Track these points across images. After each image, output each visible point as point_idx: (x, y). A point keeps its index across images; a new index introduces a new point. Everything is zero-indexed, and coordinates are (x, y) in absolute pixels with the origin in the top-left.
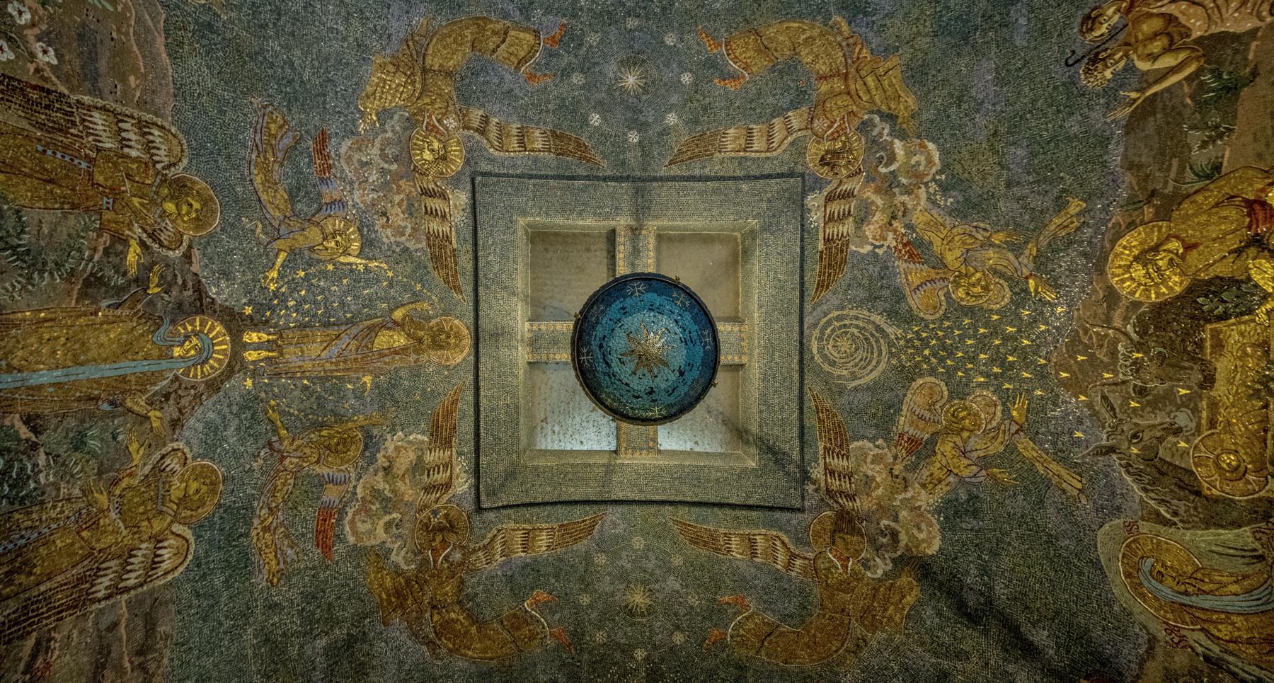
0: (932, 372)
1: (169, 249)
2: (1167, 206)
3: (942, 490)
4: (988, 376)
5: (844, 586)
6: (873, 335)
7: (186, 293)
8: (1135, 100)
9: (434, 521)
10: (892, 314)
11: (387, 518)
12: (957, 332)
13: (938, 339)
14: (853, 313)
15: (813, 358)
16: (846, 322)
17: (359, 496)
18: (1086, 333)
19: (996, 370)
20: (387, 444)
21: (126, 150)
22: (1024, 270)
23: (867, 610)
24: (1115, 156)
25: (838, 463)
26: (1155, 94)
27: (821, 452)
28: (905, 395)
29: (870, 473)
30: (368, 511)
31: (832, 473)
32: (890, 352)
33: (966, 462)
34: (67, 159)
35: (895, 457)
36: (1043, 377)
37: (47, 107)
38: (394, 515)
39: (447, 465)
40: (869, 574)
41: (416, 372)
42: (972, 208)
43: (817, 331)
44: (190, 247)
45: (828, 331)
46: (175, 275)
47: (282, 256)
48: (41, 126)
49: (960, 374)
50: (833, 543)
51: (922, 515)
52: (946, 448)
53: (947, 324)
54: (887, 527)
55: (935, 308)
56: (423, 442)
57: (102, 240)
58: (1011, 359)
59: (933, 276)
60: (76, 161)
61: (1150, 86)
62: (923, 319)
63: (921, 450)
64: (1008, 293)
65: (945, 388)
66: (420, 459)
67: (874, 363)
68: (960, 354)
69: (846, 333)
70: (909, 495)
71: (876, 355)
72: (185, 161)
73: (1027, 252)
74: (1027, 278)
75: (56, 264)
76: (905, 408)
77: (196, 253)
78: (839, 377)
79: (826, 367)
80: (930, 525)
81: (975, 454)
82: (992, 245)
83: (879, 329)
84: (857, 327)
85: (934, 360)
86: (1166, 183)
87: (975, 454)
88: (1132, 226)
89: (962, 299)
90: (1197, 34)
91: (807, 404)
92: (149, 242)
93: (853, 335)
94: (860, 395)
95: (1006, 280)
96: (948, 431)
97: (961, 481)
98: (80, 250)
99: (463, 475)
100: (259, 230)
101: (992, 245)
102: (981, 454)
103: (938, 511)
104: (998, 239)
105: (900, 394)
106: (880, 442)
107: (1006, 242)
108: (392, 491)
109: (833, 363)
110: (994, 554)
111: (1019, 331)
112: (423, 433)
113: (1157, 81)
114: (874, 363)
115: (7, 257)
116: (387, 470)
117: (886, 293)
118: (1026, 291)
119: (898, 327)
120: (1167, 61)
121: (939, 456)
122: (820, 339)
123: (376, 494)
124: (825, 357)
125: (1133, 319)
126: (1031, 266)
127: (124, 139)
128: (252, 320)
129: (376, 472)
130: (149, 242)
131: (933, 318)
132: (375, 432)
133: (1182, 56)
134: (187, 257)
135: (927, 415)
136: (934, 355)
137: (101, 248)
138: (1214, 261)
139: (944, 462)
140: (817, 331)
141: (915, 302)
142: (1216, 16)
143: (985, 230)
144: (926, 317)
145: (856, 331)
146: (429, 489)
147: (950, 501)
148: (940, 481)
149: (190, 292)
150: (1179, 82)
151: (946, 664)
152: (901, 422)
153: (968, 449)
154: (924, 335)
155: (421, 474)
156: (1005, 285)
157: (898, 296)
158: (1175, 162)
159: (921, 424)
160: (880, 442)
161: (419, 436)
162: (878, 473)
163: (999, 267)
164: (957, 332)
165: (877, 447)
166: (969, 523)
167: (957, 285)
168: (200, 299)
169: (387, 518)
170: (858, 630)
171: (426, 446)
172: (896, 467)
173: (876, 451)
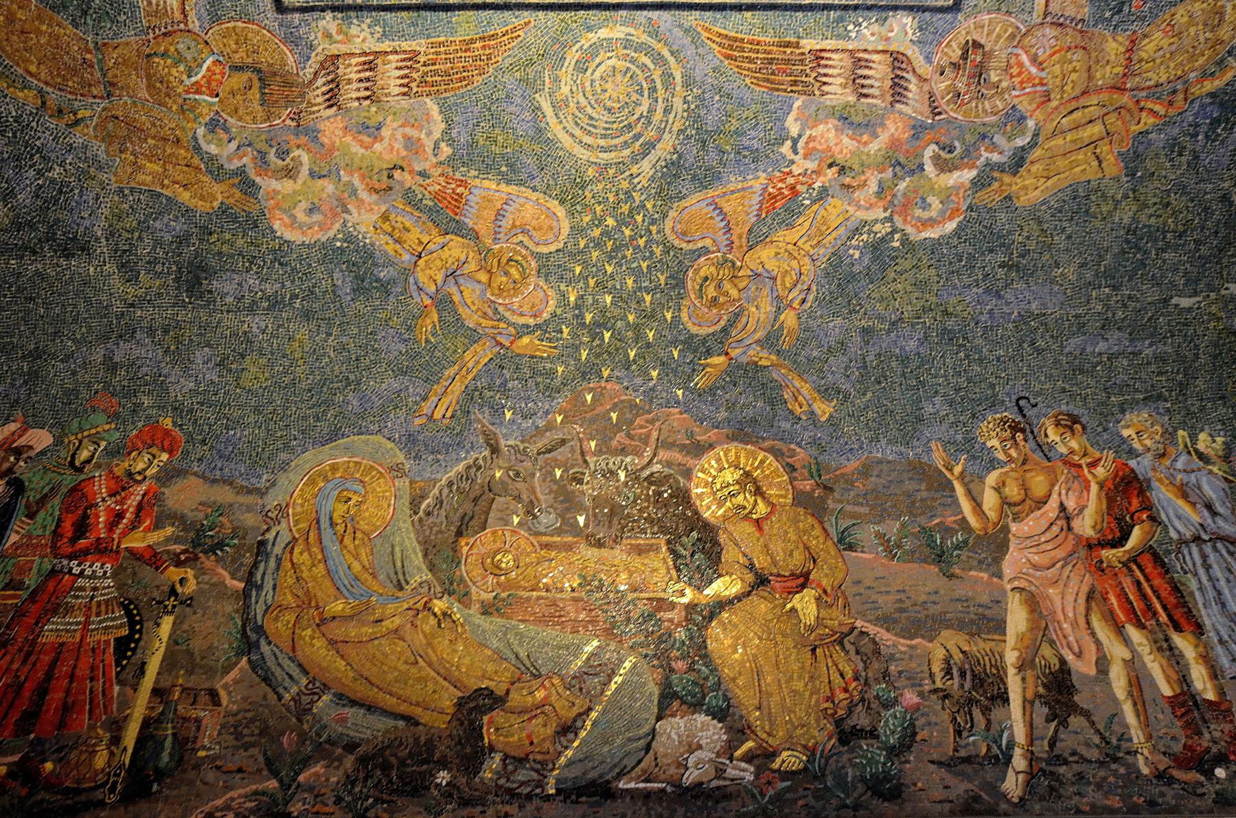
0: (577, 231)
2: (812, 504)
3: (384, 243)
4: (577, 306)
5: (160, 89)
6: (637, 137)
8: (951, 470)
10: (673, 170)
12: (644, 265)
13: (632, 238)
14: (678, 104)
15: (590, 29)
16: (661, 93)
18: (647, 421)
19: (588, 318)
22: (738, 351)
23: (134, 129)
24: (885, 451)
25: (390, 76)
26: (953, 490)
27: (406, 45)
28: (534, 189)
29: (386, 132)
31: (370, 66)
32: (607, 166)
33: (440, 278)
35: (423, 174)
36: (584, 375)
40: (201, 131)
42: (841, 282)
43: (644, 38)
45: (647, 61)
49: (578, 270)
50: (237, 68)
51: (335, 215)
52: (456, 249)
53: (658, 251)
54: (298, 162)
55: (684, 234)
58: (607, 335)
59: (736, 231)
61: (965, 485)
62: (665, 216)
63: (446, 215)
64: (704, 331)
65: (553, 248)
67: (587, 139)
68: (609, 269)
69: (640, 92)
70: (364, 195)
71: (602, 142)
73: (764, 354)
74: (727, 354)
76: (512, 189)
78: (557, 80)
79: (572, 56)
80: (323, 227)
81: (453, 289)
82: (779, 311)
83: (650, 146)
84: (651, 111)
85: (597, 232)
86: (840, 501)
87: (453, 289)
88: (790, 469)
89: (697, 271)
90: (1014, 527)
91: (497, 16)
93: (637, 104)
94: (527, 115)
95: (724, 330)
96: (485, 254)
97: (406, 273)
101: (779, 311)
102: (457, 298)
103: (349, 238)
104: (789, 319)
105: (536, 182)
106: (446, 150)
107: (781, 327)
109: (581, 67)
110: (307, 315)
111: (648, 345)
113: (969, 492)
114: (587, 139)
117: (712, 158)
118: (709, 353)
119: (652, 179)
120: (990, 501)
121: (440, 240)
122: (627, 43)
124: (594, 50)
125: (667, 471)
126: (744, 359)
131: (668, 231)
133: (992, 515)
135: (506, 223)
136: (606, 233)
138: (740, 543)
139: (431, 246)
140: (644, 38)
141: (695, 203)
142: (1028, 543)
143: (804, 301)
144: (668, 224)
145: (644, 108)
147: (371, 256)
148: (397, 241)
150: (961, 512)
151: (103, 248)
152: (486, 183)
153: (461, 281)
154: (639, 218)
156: (718, 327)
157: (706, 178)
158: (864, 510)
159: (490, 214)
160: (446, 150)
162: (388, 147)
163: (744, 320)
164: (644, 265)
165: (436, 146)
166: (343, 282)
167: (720, 265)
170: (91, 110)
172: (407, 176)
173: (429, 144)
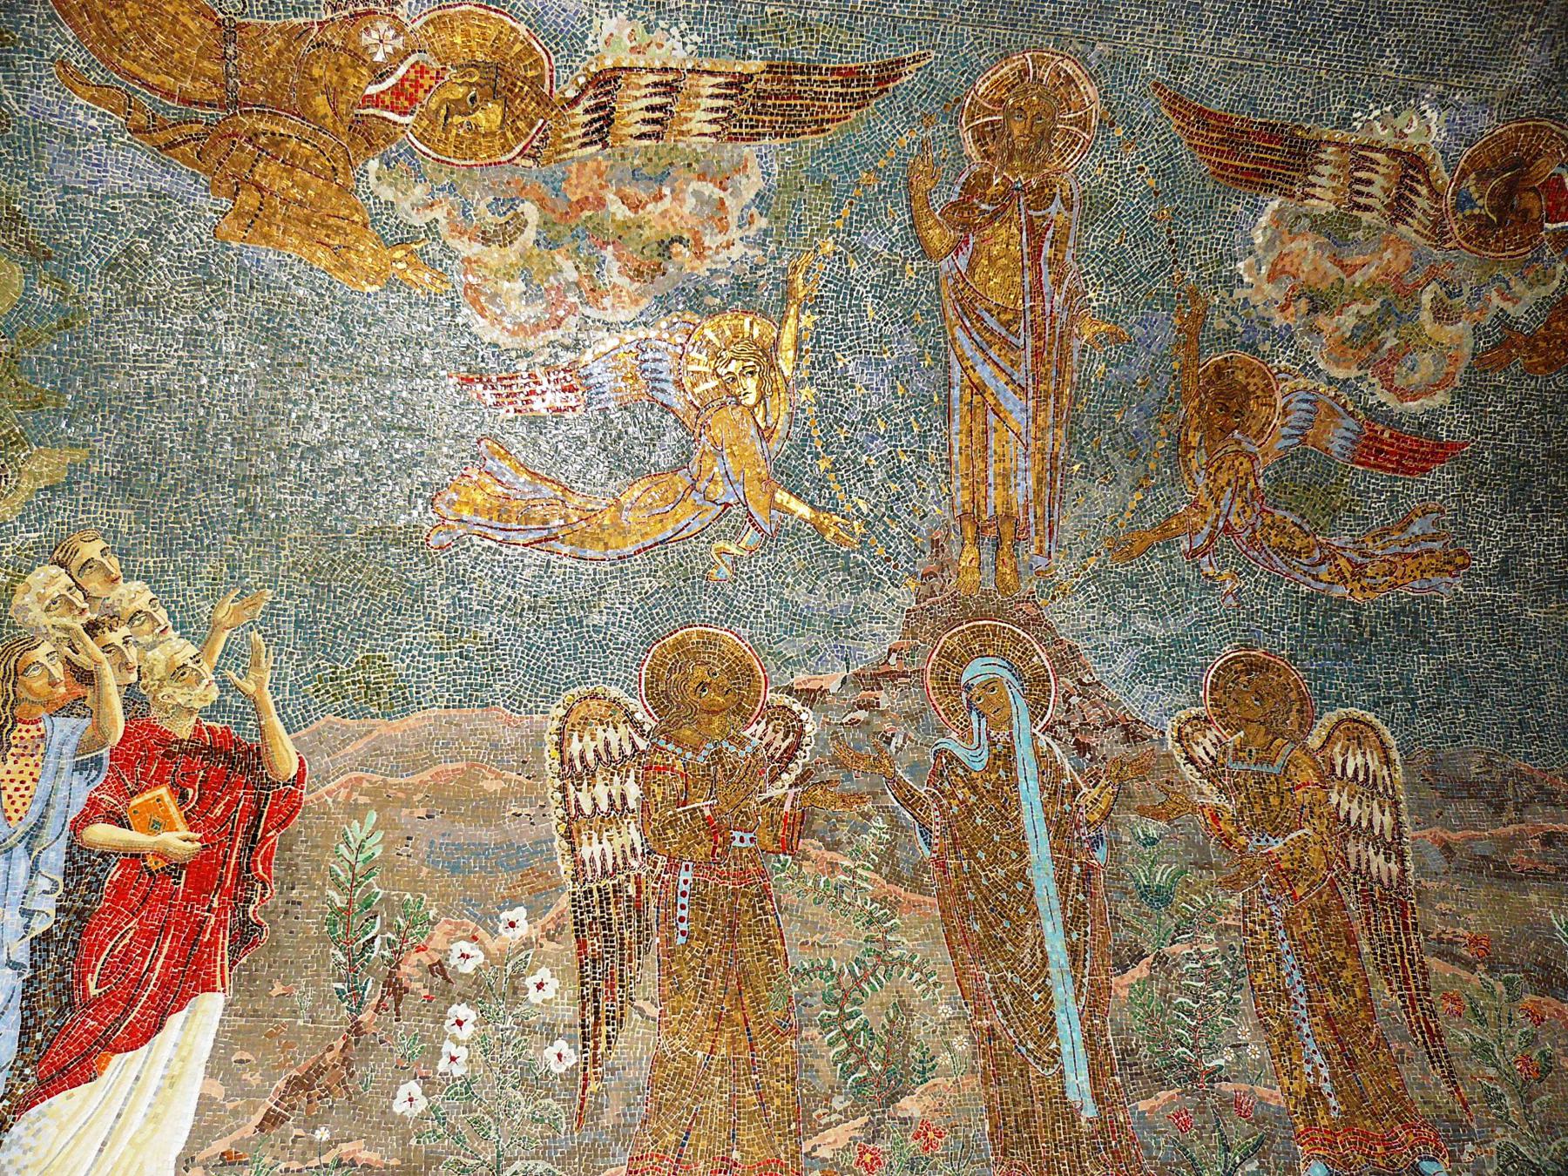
1: (801, 734)
7: (884, 706)
9: (1482, 206)
11: (1426, 316)
17: (1354, 372)
20: (1257, 299)
21: (632, 804)
30: (1395, 357)
34: (685, 901)
37: (607, 926)
38: (1426, 298)
39: (1359, 157)
41: (1095, 207)
44: (790, 691)
46: (853, 722)
47: (782, 497)
48: (643, 936)
56: (1280, 211)
57: (813, 853)
60: (682, 887)
66: (1318, 224)
72: (614, 691)
75: (870, 922)
77: (800, 678)
92: (796, 769)
98: (840, 889)
99: (1400, 122)
100: (733, 549)
108: (1368, 298)
112: (1257, 210)
115: (874, 989)
116: (1319, 304)
123: (1364, 338)
127: (612, 805)
128: (931, 575)
129: (1314, 330)
130: (796, 769)
132: (1220, 324)
134: (810, 697)
137: (829, 855)
146: (1399, 209)
149: (882, 695)
155: (1356, 224)
161: (1264, 220)
168: (892, 676)
169: (1426, 316)
171: (1291, 205)
